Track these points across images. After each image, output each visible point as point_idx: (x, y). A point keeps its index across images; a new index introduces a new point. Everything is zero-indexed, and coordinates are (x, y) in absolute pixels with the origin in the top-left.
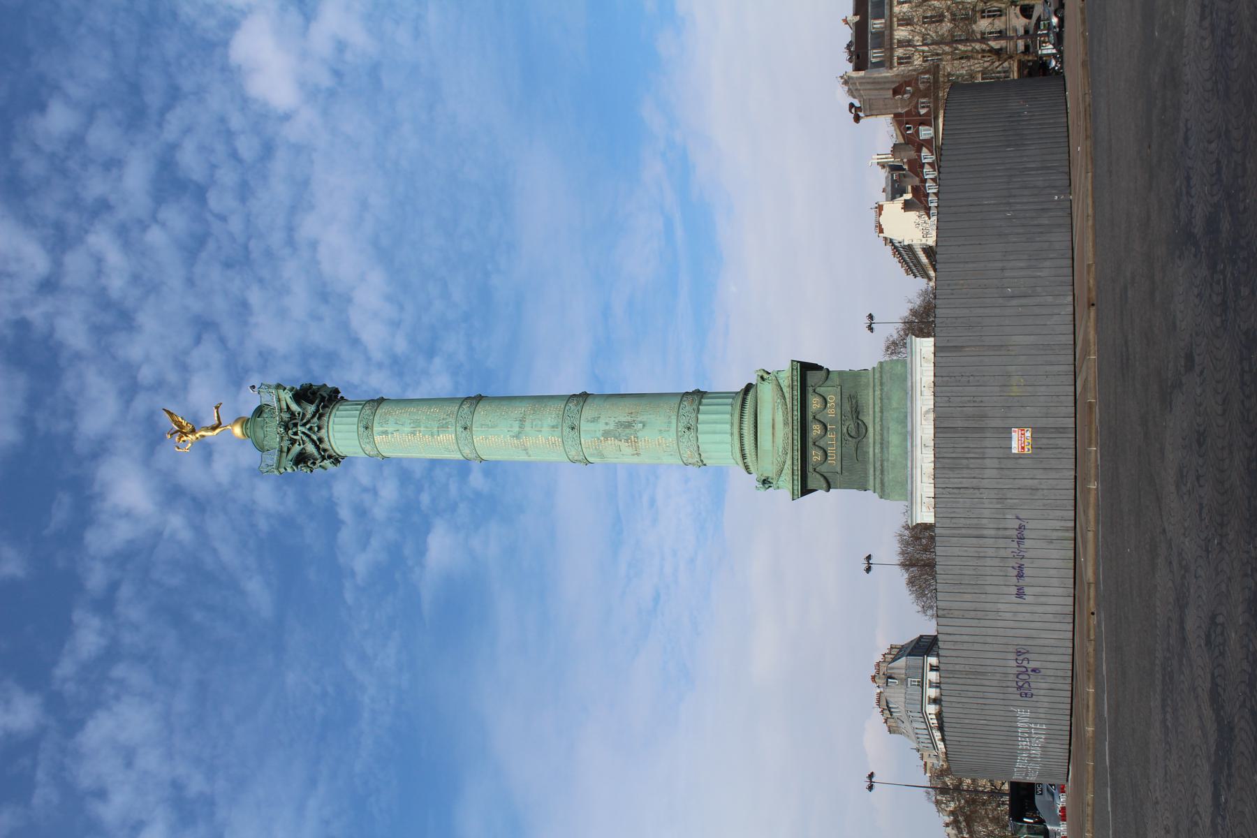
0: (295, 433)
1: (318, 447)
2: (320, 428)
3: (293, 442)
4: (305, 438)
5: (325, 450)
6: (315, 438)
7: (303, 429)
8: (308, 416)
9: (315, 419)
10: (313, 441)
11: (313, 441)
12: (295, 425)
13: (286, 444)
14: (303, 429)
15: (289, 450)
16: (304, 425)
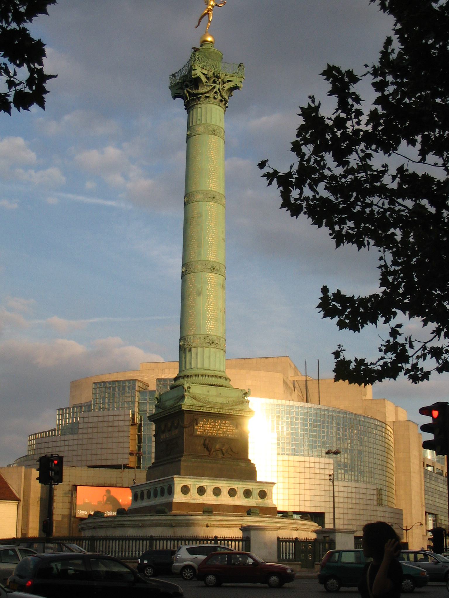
0: (214, 82)
1: (202, 94)
2: (215, 98)
3: (208, 78)
4: (211, 87)
5: (201, 97)
6: (211, 95)
7: (216, 89)
8: (223, 94)
9: (220, 98)
10: (208, 92)
11: (208, 92)
12: (219, 84)
13: (210, 74)
14: (216, 89)
15: (204, 74)
16: (219, 90)
